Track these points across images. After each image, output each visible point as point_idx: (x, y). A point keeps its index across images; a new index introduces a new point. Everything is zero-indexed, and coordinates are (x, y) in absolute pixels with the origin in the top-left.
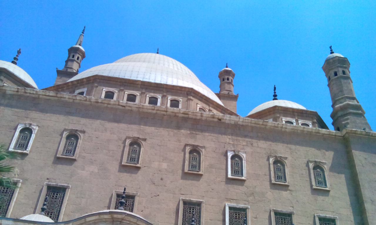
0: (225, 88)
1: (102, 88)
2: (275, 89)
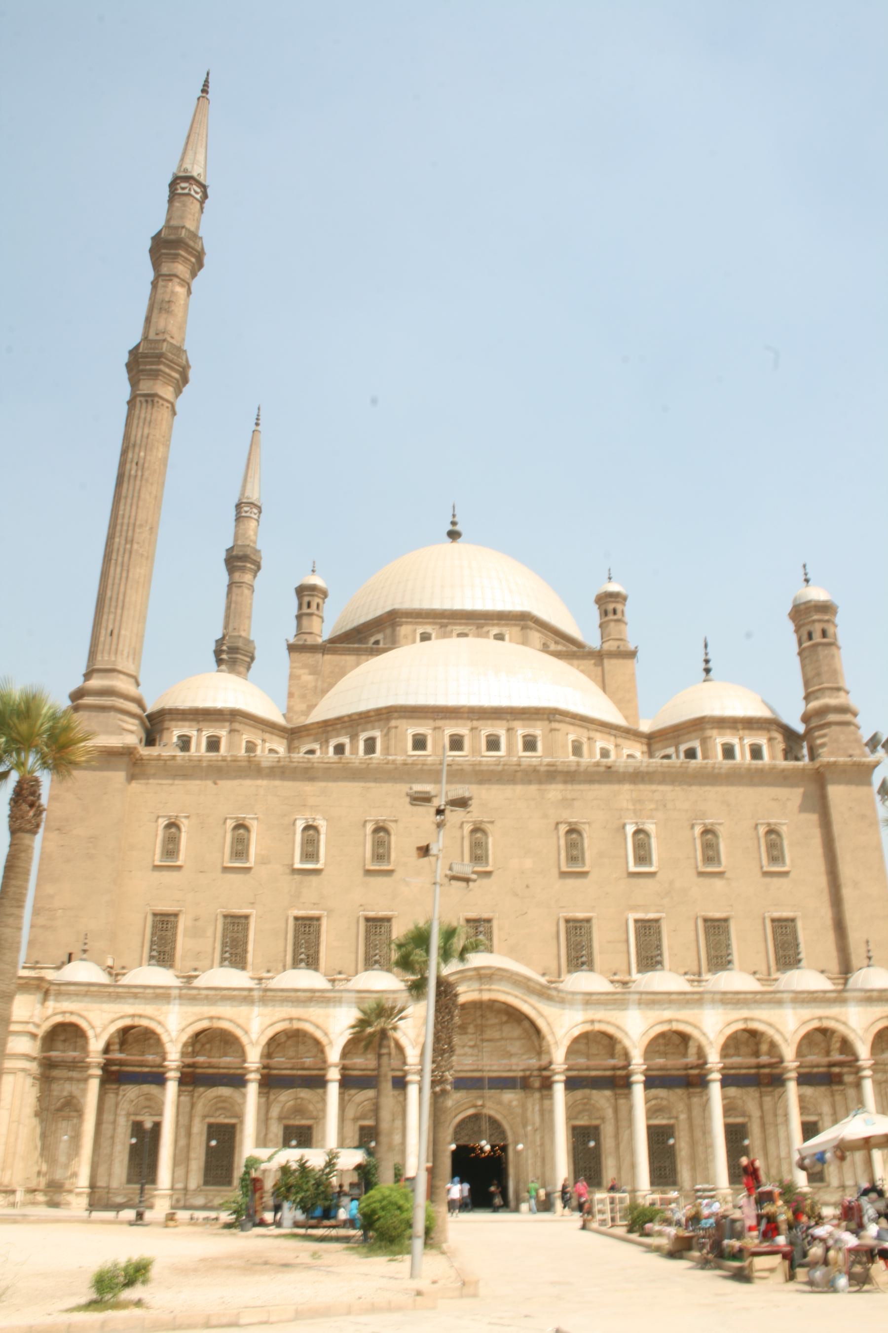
0: (609, 635)
2: (706, 646)
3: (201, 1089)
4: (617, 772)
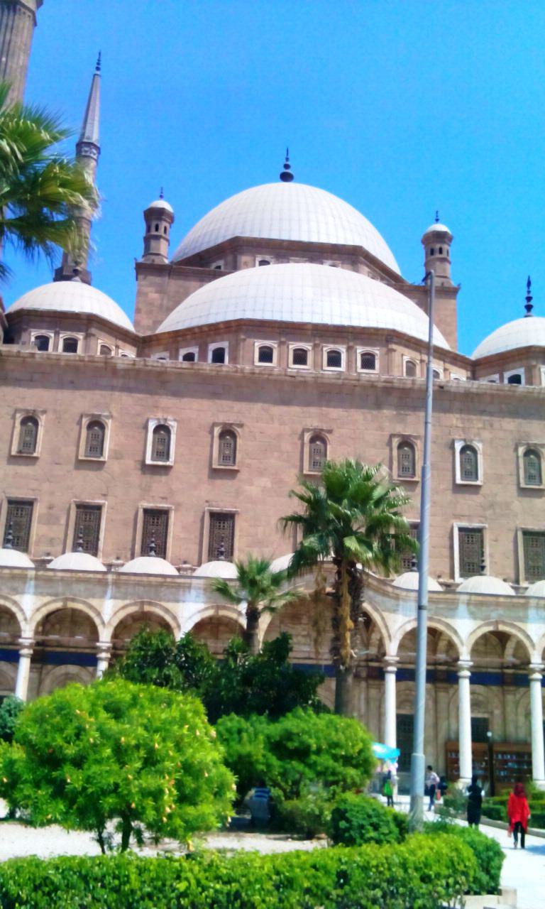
1: (251, 340)
3: (50, 667)
4: (449, 392)
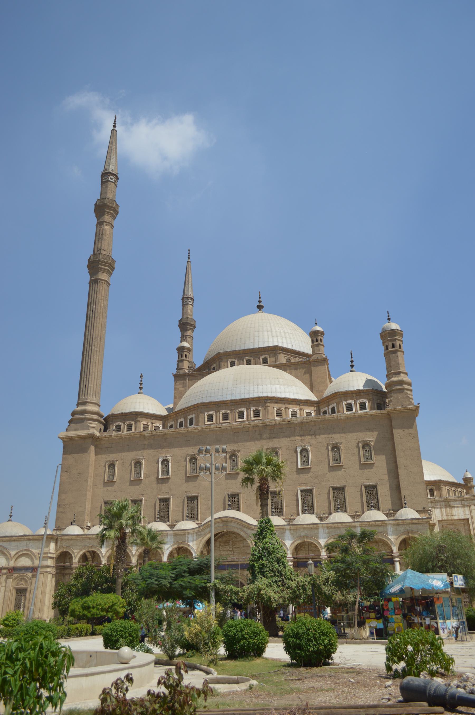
4: (293, 423)
